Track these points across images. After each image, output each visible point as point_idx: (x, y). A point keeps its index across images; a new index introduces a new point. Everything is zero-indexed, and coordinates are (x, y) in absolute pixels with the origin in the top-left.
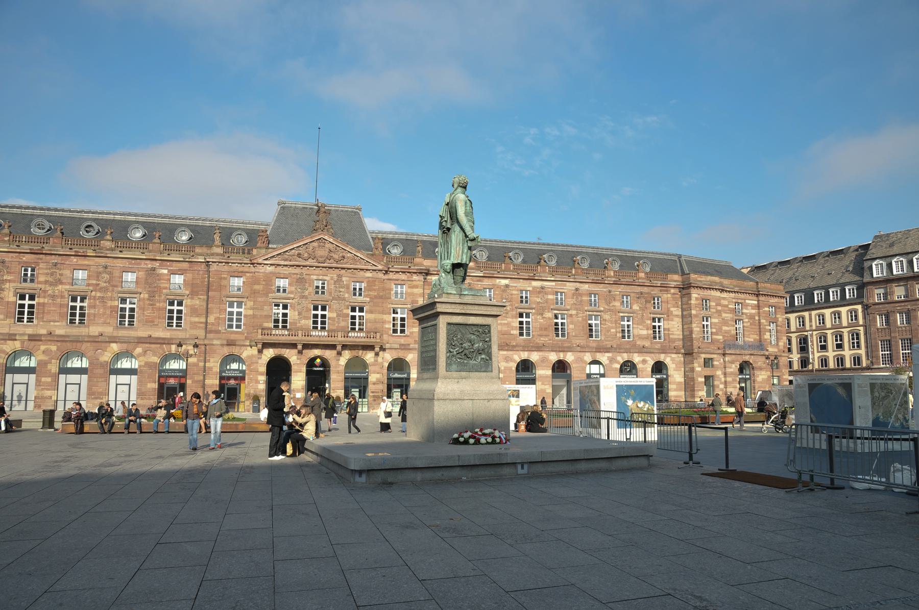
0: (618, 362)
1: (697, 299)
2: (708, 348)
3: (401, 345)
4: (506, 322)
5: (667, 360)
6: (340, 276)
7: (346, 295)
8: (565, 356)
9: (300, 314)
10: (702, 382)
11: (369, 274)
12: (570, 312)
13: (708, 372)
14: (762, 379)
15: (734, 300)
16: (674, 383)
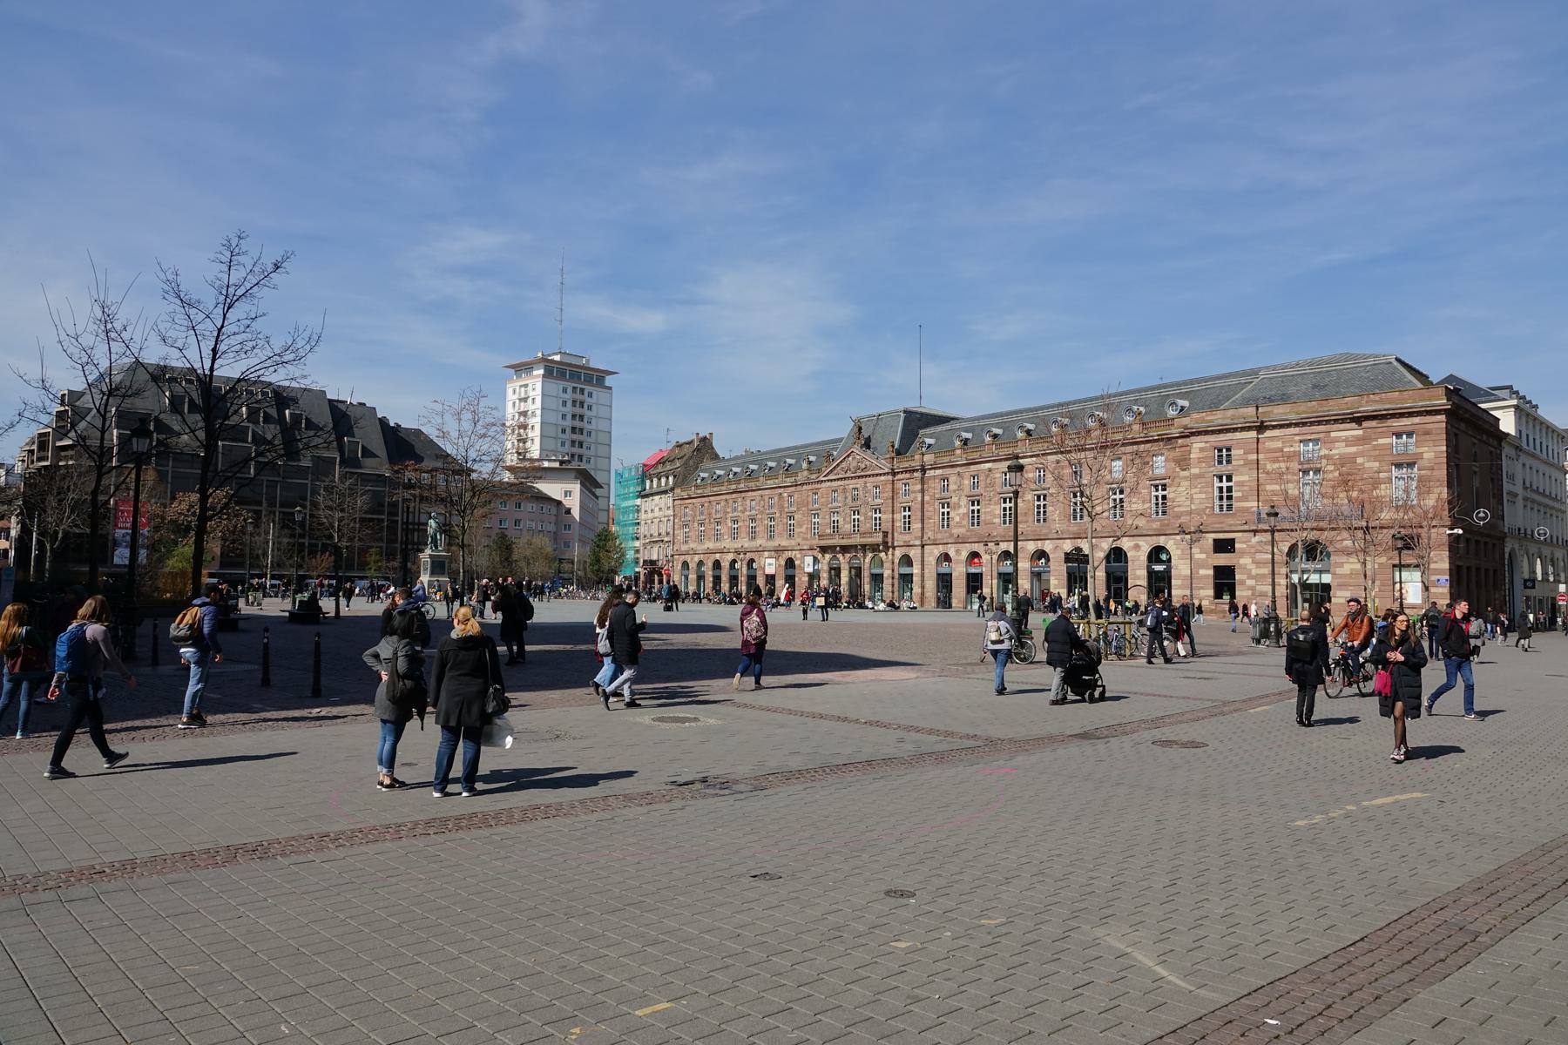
0: (1102, 550)
1: (1202, 450)
2: (1222, 523)
3: (905, 542)
4: (989, 510)
5: (1170, 544)
6: (866, 483)
7: (870, 499)
8: (1043, 546)
9: (844, 519)
10: (1209, 575)
11: (883, 478)
12: (1050, 491)
13: (1223, 559)
14: (1352, 570)
15: (1297, 438)
16: (1179, 577)
